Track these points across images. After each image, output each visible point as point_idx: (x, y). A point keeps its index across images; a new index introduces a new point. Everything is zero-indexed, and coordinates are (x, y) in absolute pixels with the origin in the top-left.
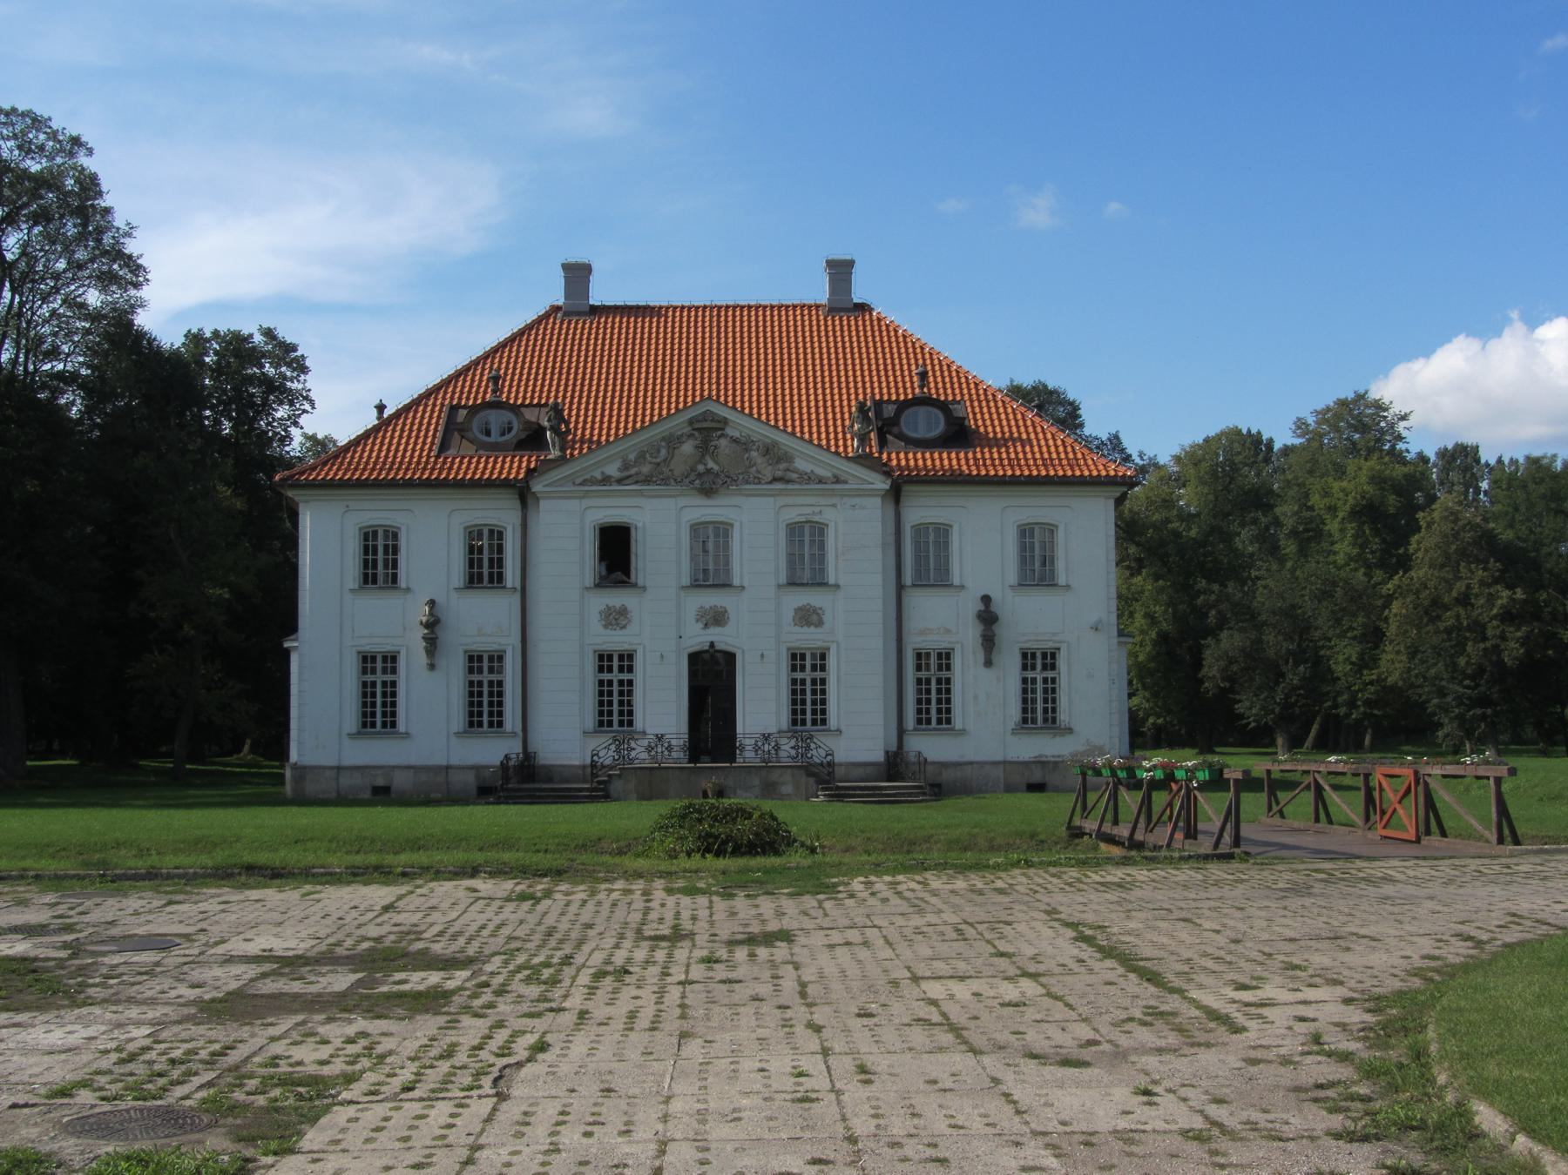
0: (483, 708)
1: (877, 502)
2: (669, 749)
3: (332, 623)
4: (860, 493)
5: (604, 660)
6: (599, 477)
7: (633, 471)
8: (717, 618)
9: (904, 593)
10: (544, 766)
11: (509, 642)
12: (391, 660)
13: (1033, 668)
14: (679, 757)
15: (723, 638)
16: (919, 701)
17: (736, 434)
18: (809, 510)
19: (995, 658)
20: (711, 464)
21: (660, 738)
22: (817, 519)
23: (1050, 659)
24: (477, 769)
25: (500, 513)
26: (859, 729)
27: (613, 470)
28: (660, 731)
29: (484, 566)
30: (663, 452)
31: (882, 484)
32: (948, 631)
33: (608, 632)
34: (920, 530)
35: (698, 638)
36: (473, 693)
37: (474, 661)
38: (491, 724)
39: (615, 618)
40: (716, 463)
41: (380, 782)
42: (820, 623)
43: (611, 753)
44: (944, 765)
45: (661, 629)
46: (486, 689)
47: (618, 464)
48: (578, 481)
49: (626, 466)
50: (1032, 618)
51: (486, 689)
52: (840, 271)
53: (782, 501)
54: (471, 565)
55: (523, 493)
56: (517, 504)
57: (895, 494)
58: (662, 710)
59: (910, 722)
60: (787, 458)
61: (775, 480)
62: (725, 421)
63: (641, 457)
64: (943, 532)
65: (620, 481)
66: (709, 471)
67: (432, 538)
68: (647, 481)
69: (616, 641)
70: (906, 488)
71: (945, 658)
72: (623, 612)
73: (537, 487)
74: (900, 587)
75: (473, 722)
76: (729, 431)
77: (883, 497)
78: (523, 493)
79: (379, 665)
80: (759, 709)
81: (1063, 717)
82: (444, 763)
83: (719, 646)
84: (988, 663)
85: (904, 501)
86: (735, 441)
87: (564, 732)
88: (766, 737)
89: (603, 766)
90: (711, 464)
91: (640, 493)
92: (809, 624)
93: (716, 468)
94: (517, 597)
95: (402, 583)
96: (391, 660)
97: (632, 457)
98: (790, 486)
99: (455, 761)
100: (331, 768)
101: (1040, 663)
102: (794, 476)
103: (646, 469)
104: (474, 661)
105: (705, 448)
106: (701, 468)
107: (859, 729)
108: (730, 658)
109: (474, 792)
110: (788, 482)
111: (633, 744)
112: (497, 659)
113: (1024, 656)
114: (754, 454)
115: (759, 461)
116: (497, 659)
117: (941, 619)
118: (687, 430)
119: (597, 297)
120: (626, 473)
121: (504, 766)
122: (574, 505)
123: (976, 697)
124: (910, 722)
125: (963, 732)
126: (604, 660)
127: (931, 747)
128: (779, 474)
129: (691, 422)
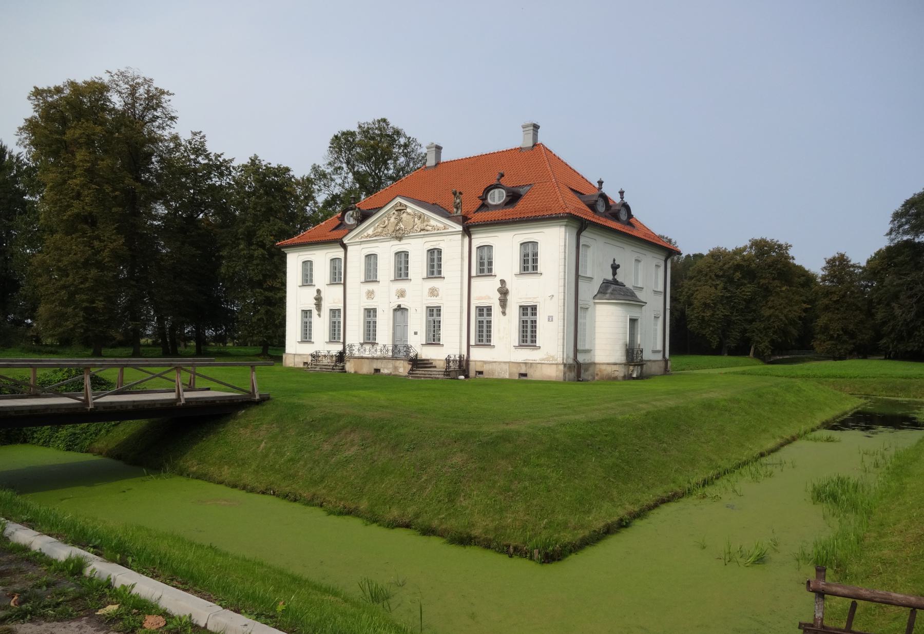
2: (387, 351)
9: (473, 280)
19: (507, 311)
21: (384, 346)
32: (489, 298)
39: (370, 294)
44: (485, 362)
47: (372, 229)
61: (423, 230)
69: (370, 304)
76: (408, 210)
84: (504, 313)
96: (310, 311)
102: (429, 228)
107: (452, 345)
117: (485, 291)
119: (444, 158)
127: (478, 355)
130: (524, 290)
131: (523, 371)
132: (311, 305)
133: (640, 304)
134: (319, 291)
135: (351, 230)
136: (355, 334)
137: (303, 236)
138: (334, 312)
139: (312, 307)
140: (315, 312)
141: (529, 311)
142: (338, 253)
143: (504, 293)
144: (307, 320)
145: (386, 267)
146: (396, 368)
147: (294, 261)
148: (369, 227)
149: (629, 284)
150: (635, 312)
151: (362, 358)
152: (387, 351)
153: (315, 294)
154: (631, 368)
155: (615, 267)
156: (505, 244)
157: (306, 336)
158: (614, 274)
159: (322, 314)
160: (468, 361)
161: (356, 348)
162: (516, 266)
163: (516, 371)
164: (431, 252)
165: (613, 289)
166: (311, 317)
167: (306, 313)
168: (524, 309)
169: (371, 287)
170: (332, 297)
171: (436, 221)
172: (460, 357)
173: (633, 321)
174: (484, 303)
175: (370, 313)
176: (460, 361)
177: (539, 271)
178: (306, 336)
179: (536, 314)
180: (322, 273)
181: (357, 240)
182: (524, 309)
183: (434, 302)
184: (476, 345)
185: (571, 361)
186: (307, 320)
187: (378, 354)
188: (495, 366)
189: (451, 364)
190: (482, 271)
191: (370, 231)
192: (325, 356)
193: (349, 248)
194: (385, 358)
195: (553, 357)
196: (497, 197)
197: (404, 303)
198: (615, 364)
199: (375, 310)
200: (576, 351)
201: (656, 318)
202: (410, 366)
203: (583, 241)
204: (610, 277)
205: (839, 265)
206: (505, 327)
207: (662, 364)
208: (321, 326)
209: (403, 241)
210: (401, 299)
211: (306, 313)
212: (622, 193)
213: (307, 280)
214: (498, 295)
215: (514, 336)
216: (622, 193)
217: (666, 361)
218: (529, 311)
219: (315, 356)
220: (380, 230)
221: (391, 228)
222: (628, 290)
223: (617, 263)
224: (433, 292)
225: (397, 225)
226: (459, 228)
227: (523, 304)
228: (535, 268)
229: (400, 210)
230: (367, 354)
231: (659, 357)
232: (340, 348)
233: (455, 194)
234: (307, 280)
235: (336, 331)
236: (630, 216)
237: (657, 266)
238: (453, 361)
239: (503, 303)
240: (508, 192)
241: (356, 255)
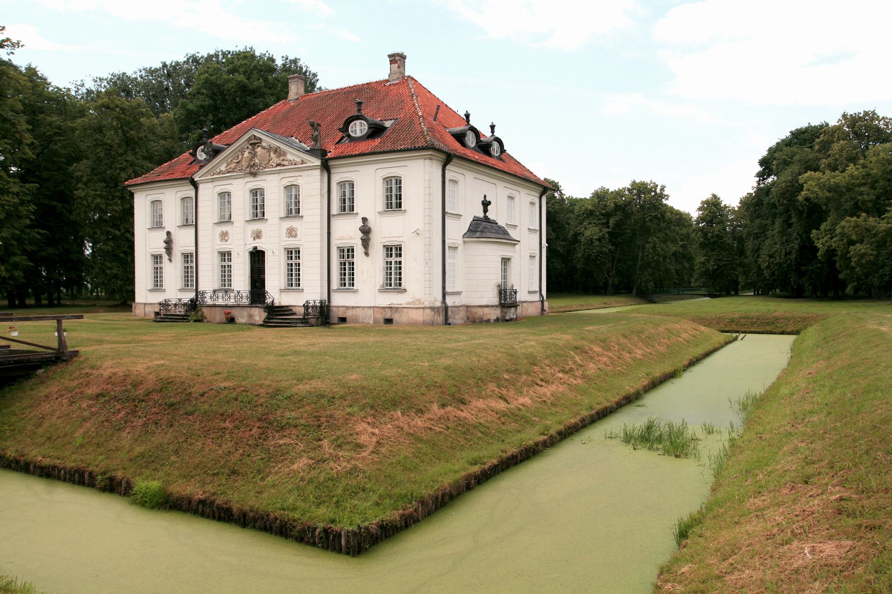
11: (192, 249)
13: (391, 256)
14: (245, 301)
18: (291, 179)
19: (370, 252)
21: (239, 292)
27: (223, 168)
34: (342, 184)
39: (224, 236)
42: (296, 236)
44: (347, 308)
47: (225, 165)
52: (397, 59)
53: (282, 175)
56: (192, 187)
59: (335, 284)
61: (278, 165)
62: (260, 139)
69: (225, 247)
70: (331, 163)
76: (264, 144)
83: (259, 249)
84: (367, 254)
85: (333, 171)
102: (286, 163)
107: (312, 291)
116: (192, 256)
117: (347, 231)
123: (362, 272)
125: (356, 291)
127: (340, 300)
130: (387, 229)
131: (388, 316)
132: (161, 249)
133: (513, 243)
134: (168, 233)
135: (201, 167)
136: (209, 281)
137: (149, 176)
138: (186, 257)
139: (163, 251)
140: (165, 257)
141: (393, 250)
142: (190, 191)
143: (366, 231)
144: (159, 266)
145: (241, 205)
147: (142, 203)
148: (221, 163)
149: (501, 223)
150: (506, 251)
151: (215, 306)
152: (242, 297)
153: (165, 237)
154: (505, 310)
155: (486, 204)
156: (367, 180)
157: (158, 283)
158: (485, 211)
159: (173, 259)
160: (329, 306)
161: (208, 296)
162: (380, 204)
163: (380, 317)
165: (484, 228)
166: (161, 262)
167: (157, 258)
168: (388, 249)
169: (224, 228)
170: (184, 241)
171: (293, 155)
172: (321, 302)
173: (505, 261)
174: (346, 243)
175: (225, 256)
176: (321, 307)
177: (403, 209)
178: (158, 283)
179: (400, 255)
180: (172, 215)
181: (209, 177)
182: (388, 249)
183: (292, 243)
184: (338, 290)
185: (438, 304)
186: (159, 266)
187: (232, 302)
188: (358, 312)
189: (310, 310)
191: (223, 168)
192: (175, 305)
193: (201, 187)
194: (239, 306)
195: (419, 300)
196: (359, 129)
197: (261, 245)
198: (487, 306)
199: (229, 254)
200: (444, 294)
201: (532, 257)
202: (266, 314)
203: (449, 175)
204: (481, 215)
205: (713, 207)
206: (369, 270)
207: (539, 305)
208: (173, 272)
209: (258, 178)
210: (257, 240)
211: (157, 258)
212: (493, 127)
213: (157, 224)
214: (361, 235)
215: (379, 278)
216: (493, 127)
217: (542, 302)
218: (393, 250)
219: (165, 305)
220: (233, 166)
221: (244, 163)
222: (500, 227)
223: (488, 199)
225: (251, 160)
226: (318, 162)
227: (386, 244)
228: (399, 205)
229: (255, 144)
230: (220, 302)
231: (536, 297)
232: (192, 295)
233: (312, 125)
234: (157, 224)
235: (191, 275)
236: (503, 151)
237: (532, 204)
238: (313, 307)
239: (366, 243)
240: (369, 124)
241: (208, 194)
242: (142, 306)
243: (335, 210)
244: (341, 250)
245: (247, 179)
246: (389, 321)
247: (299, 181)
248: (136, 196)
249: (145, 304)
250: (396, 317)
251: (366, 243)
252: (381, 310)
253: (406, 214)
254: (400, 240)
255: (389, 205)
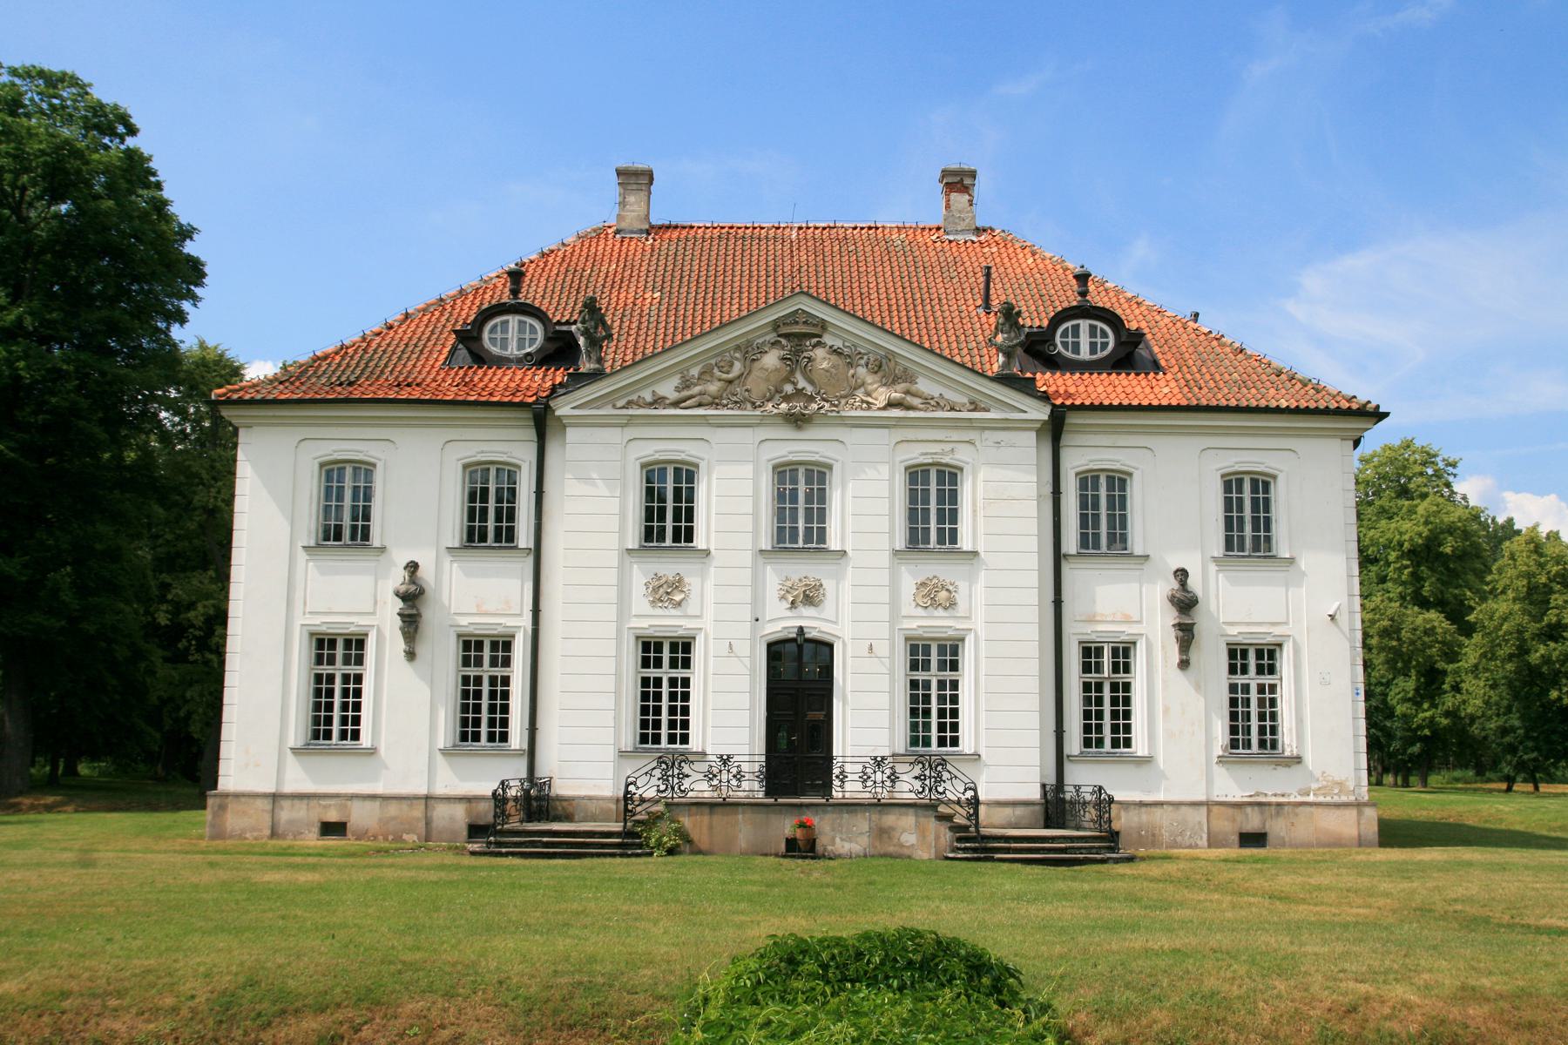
0: (481, 714)
1: (1033, 434)
2: (739, 776)
3: (276, 590)
4: (1006, 426)
5: (650, 650)
6: (649, 398)
7: (696, 390)
8: (809, 597)
10: (560, 799)
12: (356, 645)
13: (1244, 670)
14: (752, 788)
15: (815, 623)
16: (1087, 715)
17: (838, 344)
20: (802, 383)
21: (725, 760)
22: (946, 460)
23: (1267, 658)
24: (468, 800)
25: (510, 445)
26: (1005, 758)
27: (668, 389)
28: (725, 751)
29: (490, 519)
30: (738, 368)
31: (1041, 413)
33: (659, 612)
34: (1088, 481)
35: (782, 622)
36: (469, 691)
37: (471, 647)
38: (491, 737)
40: (811, 382)
41: (333, 816)
42: (952, 604)
43: (654, 781)
45: (730, 616)
46: (486, 688)
47: (676, 380)
48: (619, 404)
49: (686, 384)
50: (1238, 604)
51: (486, 688)
54: (471, 518)
55: (542, 421)
56: (531, 434)
57: (1055, 429)
58: (729, 718)
59: (1074, 743)
60: (907, 377)
61: (891, 405)
62: (823, 325)
63: (706, 374)
64: (1118, 482)
65: (676, 404)
66: (799, 393)
67: (420, 478)
68: (715, 402)
70: (1073, 419)
71: (1123, 655)
72: (677, 584)
73: (563, 408)
74: (1058, 557)
75: (468, 732)
76: (828, 339)
77: (1039, 432)
78: (542, 421)
79: (340, 651)
80: (865, 722)
81: (1288, 739)
82: (423, 791)
83: (811, 634)
85: (1066, 439)
86: (836, 352)
87: (585, 750)
88: (879, 762)
89: (643, 800)
90: (802, 383)
91: (704, 421)
92: (935, 604)
93: (809, 389)
94: (530, 560)
95: (376, 540)
97: (695, 372)
98: (912, 414)
99: (440, 790)
100: (265, 796)
101: (1254, 660)
102: (916, 402)
103: (713, 388)
104: (471, 647)
105: (795, 361)
106: (789, 388)
107: (1005, 758)
108: (825, 648)
109: (465, 833)
110: (909, 408)
111: (686, 770)
112: (503, 646)
113: (1232, 654)
114: (862, 371)
115: (869, 379)
116: (503, 646)
118: (772, 337)
120: (686, 393)
121: (499, 799)
122: (614, 435)
124: (1074, 743)
126: (650, 650)
128: (896, 395)
129: (776, 325)
141: (1254, 660)
146: (882, 833)
159: (421, 650)
163: (1228, 826)
164: (652, 474)
168: (1237, 656)
174: (1105, 630)
182: (1237, 656)
190: (1088, 541)
224: (934, 595)
242: (265, 805)
243: (1071, 543)
244: (1090, 653)
245: (764, 433)
246: (1252, 839)
247: (959, 455)
248: (243, 437)
249: (275, 797)
250: (1277, 828)
251: (411, 623)
252: (1230, 811)
253: (382, 558)
254: (1277, 631)
255: (651, 534)
